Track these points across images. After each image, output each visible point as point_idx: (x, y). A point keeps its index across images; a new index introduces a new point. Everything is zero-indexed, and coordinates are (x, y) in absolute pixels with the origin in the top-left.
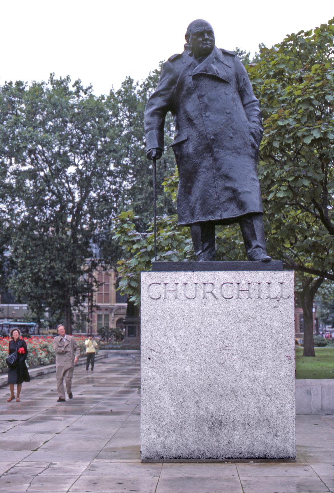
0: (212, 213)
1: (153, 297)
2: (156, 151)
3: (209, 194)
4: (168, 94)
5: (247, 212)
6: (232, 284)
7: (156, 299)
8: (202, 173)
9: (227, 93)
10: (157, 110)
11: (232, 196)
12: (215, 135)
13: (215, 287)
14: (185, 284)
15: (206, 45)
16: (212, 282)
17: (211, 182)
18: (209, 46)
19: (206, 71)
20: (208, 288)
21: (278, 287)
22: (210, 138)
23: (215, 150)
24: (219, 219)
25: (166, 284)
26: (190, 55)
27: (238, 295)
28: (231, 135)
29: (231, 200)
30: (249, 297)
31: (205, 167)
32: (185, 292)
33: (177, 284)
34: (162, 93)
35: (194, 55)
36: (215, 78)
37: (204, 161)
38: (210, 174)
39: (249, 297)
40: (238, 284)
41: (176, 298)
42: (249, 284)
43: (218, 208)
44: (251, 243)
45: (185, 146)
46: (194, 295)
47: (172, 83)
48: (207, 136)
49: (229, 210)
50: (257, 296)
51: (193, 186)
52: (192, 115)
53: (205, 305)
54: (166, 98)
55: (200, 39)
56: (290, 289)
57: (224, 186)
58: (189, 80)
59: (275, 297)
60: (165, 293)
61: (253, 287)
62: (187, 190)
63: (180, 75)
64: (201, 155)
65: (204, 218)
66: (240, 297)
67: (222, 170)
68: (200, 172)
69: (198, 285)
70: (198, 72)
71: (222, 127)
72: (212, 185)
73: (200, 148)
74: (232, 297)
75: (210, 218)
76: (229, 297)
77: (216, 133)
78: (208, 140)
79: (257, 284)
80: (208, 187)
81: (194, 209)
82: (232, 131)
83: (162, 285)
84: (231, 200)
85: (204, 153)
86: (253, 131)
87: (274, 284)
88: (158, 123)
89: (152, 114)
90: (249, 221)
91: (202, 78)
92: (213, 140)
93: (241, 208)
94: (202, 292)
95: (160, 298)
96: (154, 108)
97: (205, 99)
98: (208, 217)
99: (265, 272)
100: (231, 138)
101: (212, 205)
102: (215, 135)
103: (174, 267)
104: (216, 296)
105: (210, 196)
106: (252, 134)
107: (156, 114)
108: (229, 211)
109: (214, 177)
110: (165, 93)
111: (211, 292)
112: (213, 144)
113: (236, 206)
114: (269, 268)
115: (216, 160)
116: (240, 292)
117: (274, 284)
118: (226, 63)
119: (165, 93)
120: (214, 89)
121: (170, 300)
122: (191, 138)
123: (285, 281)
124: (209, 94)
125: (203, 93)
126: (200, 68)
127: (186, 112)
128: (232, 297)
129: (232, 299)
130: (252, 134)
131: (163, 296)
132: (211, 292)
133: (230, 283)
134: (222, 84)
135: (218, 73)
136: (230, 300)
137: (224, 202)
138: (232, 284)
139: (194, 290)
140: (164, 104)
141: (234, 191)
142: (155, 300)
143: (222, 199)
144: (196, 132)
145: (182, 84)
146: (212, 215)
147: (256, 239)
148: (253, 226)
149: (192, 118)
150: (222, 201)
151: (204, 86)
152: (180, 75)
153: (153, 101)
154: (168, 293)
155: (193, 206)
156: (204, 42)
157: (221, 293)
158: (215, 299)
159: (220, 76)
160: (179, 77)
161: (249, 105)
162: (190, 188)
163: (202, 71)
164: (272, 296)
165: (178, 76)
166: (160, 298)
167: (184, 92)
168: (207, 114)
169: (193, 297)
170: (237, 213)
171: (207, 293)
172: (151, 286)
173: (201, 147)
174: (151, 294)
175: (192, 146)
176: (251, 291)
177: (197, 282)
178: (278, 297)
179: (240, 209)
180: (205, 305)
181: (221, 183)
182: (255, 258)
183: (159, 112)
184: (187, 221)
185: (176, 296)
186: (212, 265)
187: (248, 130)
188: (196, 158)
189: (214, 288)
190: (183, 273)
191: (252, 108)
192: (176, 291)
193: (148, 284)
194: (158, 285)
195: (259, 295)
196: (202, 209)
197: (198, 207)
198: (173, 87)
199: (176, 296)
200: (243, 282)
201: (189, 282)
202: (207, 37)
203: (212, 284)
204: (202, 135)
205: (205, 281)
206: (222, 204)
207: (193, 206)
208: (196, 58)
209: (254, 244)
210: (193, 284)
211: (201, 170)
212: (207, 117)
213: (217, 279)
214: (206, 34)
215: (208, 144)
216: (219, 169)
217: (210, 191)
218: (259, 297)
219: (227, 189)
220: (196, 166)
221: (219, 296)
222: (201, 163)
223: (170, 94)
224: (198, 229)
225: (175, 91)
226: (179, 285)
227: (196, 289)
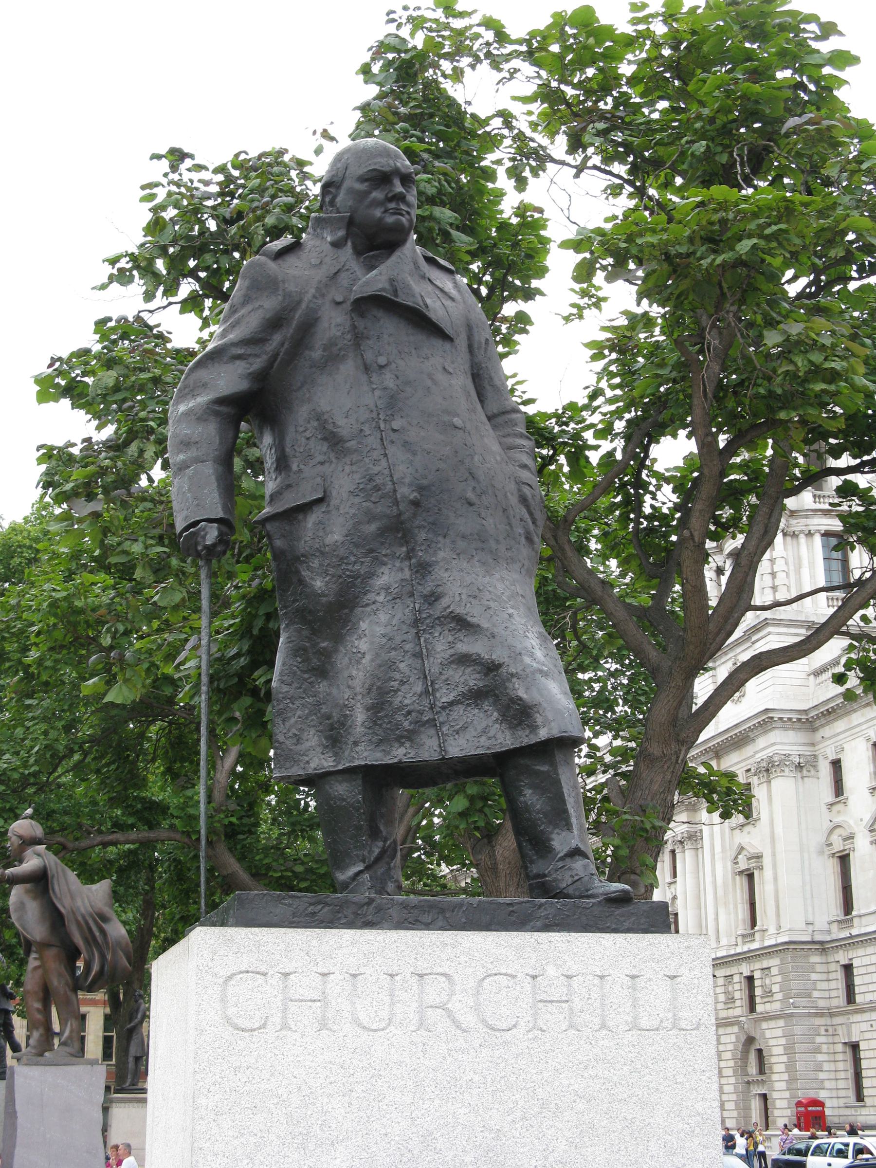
0: (409, 739)
1: (241, 1022)
3: (397, 676)
4: (256, 356)
5: (543, 734)
6: (513, 977)
7: (251, 1030)
8: (373, 606)
9: (451, 370)
10: (221, 401)
11: (481, 684)
12: (421, 489)
13: (457, 988)
14: (354, 976)
15: (395, 214)
16: (447, 971)
17: (405, 637)
18: (404, 219)
19: (395, 292)
20: (434, 991)
22: (404, 497)
23: (422, 535)
24: (436, 757)
25: (286, 975)
26: (337, 245)
27: (535, 1016)
28: (470, 495)
29: (476, 696)
30: (571, 1026)
31: (387, 589)
33: (325, 975)
34: (240, 351)
35: (349, 243)
36: (419, 320)
37: (384, 569)
38: (403, 612)
39: (571, 1026)
40: (534, 977)
41: (323, 1025)
42: (569, 977)
43: (432, 723)
44: (550, 840)
45: (312, 519)
46: (385, 1014)
47: (275, 323)
48: (395, 491)
49: (471, 729)
50: (598, 1020)
51: (336, 651)
52: (341, 422)
53: (424, 1052)
54: (251, 370)
55: (378, 195)
56: (700, 998)
57: (452, 652)
59: (655, 1023)
60: (285, 1010)
62: (315, 662)
63: (308, 297)
64: (371, 551)
65: (379, 755)
66: (541, 1023)
67: (444, 602)
68: (367, 605)
69: (397, 978)
70: (369, 291)
71: (442, 465)
72: (408, 647)
73: (372, 528)
75: (400, 754)
76: (504, 1027)
77: (425, 482)
78: (396, 503)
79: (597, 981)
80: (393, 653)
81: (343, 724)
82: (472, 483)
83: (275, 980)
84: (476, 696)
85: (382, 544)
86: (526, 490)
87: (650, 980)
88: (221, 443)
89: (200, 416)
90: (545, 768)
91: (380, 314)
92: (416, 504)
93: (519, 724)
95: (264, 1026)
96: (203, 399)
97: (389, 380)
98: (395, 753)
99: (620, 939)
100: (471, 504)
101: (409, 713)
102: (421, 489)
103: (314, 914)
104: (461, 1019)
105: (403, 683)
106: (524, 500)
107: (217, 414)
108: (471, 732)
109: (416, 622)
110: (249, 351)
111: (442, 1007)
112: (415, 515)
113: (495, 714)
114: (627, 924)
115: (423, 569)
116: (540, 1005)
117: (650, 980)
118: (438, 283)
119: (249, 351)
120: (414, 351)
121: (303, 1036)
122: (334, 493)
123: (684, 970)
124: (401, 363)
125: (382, 360)
126: (375, 280)
128: (515, 1026)
129: (515, 1030)
130: (524, 500)
131: (277, 1019)
132: (442, 1007)
133: (506, 975)
135: (427, 307)
137: (452, 704)
138: (513, 977)
139: (387, 999)
140: (243, 386)
141: (491, 668)
142: (246, 1034)
143: (445, 696)
144: (357, 477)
145: (308, 327)
146: (407, 744)
147: (568, 826)
148: (558, 782)
149: (344, 432)
150: (444, 700)
151: (385, 336)
152: (308, 297)
153: (203, 374)
154: (293, 1007)
155: (336, 716)
156: (392, 205)
158: (459, 1031)
159: (432, 316)
160: (303, 306)
161: (500, 420)
162: (326, 655)
163: (383, 289)
164: (644, 1023)
165: (299, 302)
166: (264, 1026)
167: (317, 354)
168: (396, 425)
169: (383, 1025)
170: (504, 739)
171: (430, 1011)
172: (233, 982)
174: (231, 1011)
175: (341, 520)
176: (577, 1004)
177: (395, 969)
179: (513, 727)
180: (424, 1052)
181: (441, 645)
182: (570, 890)
183: (224, 409)
184: (313, 765)
185: (324, 1018)
186: (442, 911)
187: (512, 486)
188: (353, 559)
189: (452, 994)
190: (347, 935)
191: (508, 430)
192: (323, 1000)
193: (224, 972)
194: (260, 979)
196: (374, 722)
197: (360, 716)
198: (277, 338)
199: (324, 1018)
200: (551, 971)
201: (368, 971)
202: (399, 188)
203: (444, 975)
204: (377, 488)
205: (423, 966)
206: (443, 708)
207: (336, 716)
208: (358, 252)
209: (561, 842)
211: (371, 596)
212: (394, 431)
213: (463, 959)
214: (397, 182)
216: (433, 598)
217: (402, 666)
218: (603, 1026)
219: (464, 660)
220: (354, 585)
221: (469, 1019)
222: (371, 575)
223: (265, 357)
225: (283, 350)
226: (331, 977)
227: (392, 995)
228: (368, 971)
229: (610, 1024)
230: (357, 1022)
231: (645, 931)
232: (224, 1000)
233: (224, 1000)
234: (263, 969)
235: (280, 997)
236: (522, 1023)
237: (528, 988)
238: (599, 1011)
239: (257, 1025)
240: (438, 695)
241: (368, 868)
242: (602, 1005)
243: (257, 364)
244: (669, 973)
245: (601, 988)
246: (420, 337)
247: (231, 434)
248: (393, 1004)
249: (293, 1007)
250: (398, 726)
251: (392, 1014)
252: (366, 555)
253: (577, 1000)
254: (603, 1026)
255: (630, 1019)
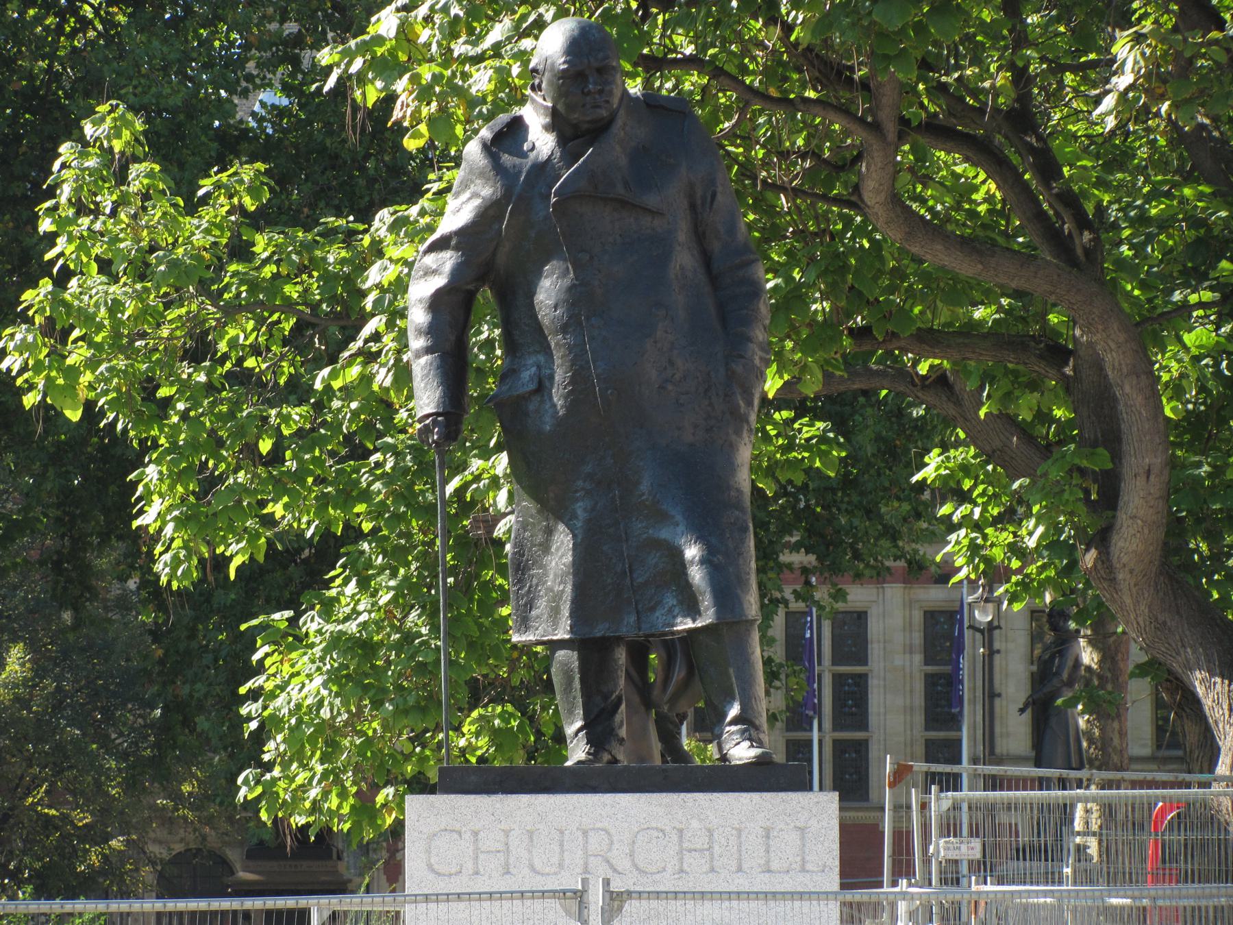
7: (451, 875)
21: (794, 837)
27: (681, 860)
30: (712, 870)
32: (530, 852)
46: (555, 860)
50: (734, 866)
61: (723, 841)
74: (664, 870)
79: (734, 832)
83: (467, 836)
94: (580, 852)
99: (756, 797)
131: (469, 866)
136: (658, 877)
139: (557, 849)
150: (640, 580)
157: (632, 855)
178: (794, 866)
185: (507, 864)
189: (612, 843)
190: (525, 798)
192: (508, 851)
194: (456, 836)
195: (740, 860)
201: (541, 827)
210: (553, 831)
213: (620, 816)
218: (740, 869)
227: (561, 845)
228: (541, 827)
229: (745, 866)
230: (532, 868)
232: (428, 851)
233: (428, 851)
234: (457, 827)
235: (472, 848)
236: (669, 866)
237: (675, 838)
238: (736, 856)
239: (453, 871)
240: (635, 576)
242: (739, 851)
244: (798, 824)
245: (739, 836)
248: (562, 851)
249: (481, 856)
251: (562, 860)
253: (716, 848)
254: (740, 869)
255: (762, 862)
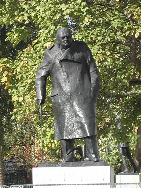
2: (41, 101)
31: (67, 110)
58: (58, 62)
75: (70, 137)
88: (42, 84)
115: (72, 106)
127: (57, 79)
134: (75, 64)
137: (77, 129)
140: (46, 74)
145: (54, 64)
173: (65, 99)
183: (42, 78)
215: (68, 97)
224: (64, 142)
231: (100, 166)
241: (67, 155)
243: (48, 70)
246: (73, 63)
247: (44, 82)
250: (69, 133)
252: (63, 104)
